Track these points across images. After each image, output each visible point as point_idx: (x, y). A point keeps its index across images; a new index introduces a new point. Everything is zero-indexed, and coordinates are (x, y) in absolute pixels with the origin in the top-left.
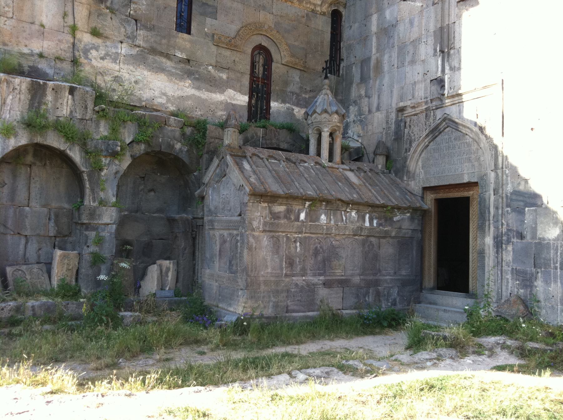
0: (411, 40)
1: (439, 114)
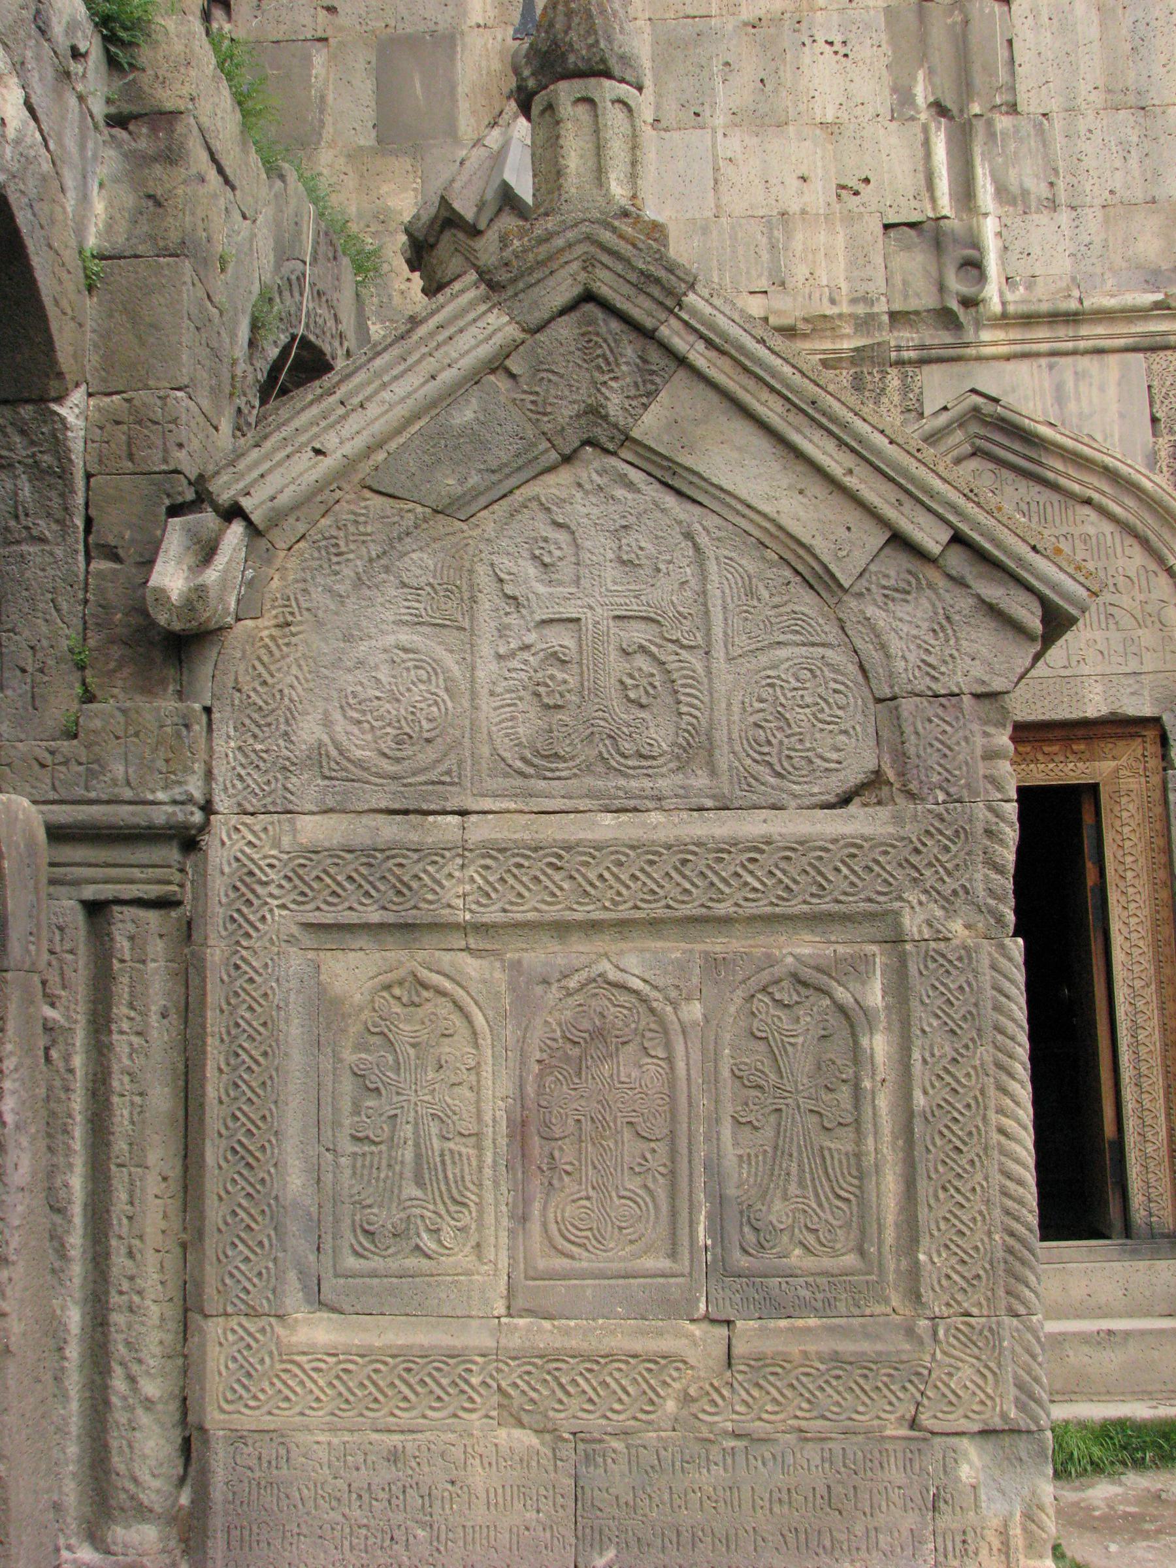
0: (746, 14)
1: (939, 389)
